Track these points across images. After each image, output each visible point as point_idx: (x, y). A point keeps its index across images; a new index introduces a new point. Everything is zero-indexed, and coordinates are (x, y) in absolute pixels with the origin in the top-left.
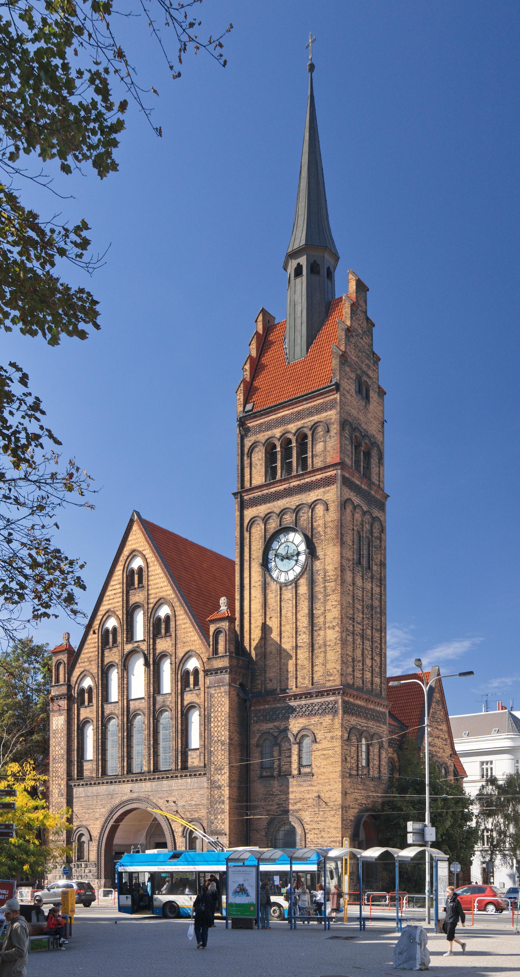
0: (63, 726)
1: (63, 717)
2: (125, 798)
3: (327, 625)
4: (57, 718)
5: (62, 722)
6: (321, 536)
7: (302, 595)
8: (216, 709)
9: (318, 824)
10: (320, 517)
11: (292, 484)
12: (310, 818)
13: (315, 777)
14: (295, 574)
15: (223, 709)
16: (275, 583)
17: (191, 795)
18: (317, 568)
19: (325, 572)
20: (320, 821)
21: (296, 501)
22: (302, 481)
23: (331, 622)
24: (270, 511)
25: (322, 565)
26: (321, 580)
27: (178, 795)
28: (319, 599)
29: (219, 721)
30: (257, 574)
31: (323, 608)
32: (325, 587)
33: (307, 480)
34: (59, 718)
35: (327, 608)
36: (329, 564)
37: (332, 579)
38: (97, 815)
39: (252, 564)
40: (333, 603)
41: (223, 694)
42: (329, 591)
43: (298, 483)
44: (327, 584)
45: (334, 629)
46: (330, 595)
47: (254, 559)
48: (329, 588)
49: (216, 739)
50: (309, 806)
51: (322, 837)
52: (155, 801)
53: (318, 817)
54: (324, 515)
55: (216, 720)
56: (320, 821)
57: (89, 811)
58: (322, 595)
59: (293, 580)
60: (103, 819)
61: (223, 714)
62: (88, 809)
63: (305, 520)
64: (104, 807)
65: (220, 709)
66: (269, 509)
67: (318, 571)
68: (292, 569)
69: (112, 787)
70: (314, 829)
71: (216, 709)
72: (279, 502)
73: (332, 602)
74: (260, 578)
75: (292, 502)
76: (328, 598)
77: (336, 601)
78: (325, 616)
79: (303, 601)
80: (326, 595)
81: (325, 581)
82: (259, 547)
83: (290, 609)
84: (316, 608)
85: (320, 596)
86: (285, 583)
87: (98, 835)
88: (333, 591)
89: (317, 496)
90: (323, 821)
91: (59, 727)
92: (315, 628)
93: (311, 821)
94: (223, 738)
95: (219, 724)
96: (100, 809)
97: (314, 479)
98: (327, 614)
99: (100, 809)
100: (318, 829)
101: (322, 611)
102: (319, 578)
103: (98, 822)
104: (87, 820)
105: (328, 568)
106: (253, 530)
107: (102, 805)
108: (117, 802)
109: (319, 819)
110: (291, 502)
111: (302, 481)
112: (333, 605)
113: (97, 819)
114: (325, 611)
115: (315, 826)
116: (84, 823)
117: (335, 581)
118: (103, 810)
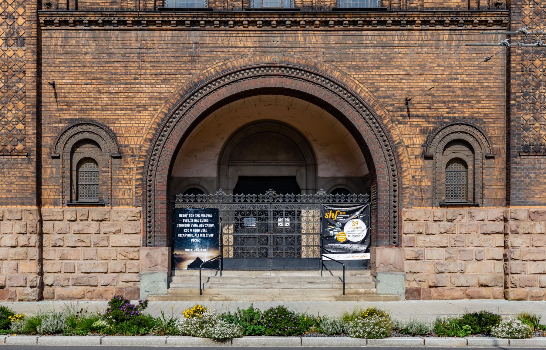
2: (239, 63)
17: (451, 66)
27: (411, 65)
38: (144, 100)
52: (336, 74)
57: (113, 88)
60: (163, 109)
62: (109, 83)
64: (165, 81)
87: (147, 146)
96: (151, 84)
99: (151, 84)
103: (145, 115)
104: (103, 109)
107: (158, 75)
108: (212, 70)
113: (143, 108)
116: (95, 115)
118: (164, 88)
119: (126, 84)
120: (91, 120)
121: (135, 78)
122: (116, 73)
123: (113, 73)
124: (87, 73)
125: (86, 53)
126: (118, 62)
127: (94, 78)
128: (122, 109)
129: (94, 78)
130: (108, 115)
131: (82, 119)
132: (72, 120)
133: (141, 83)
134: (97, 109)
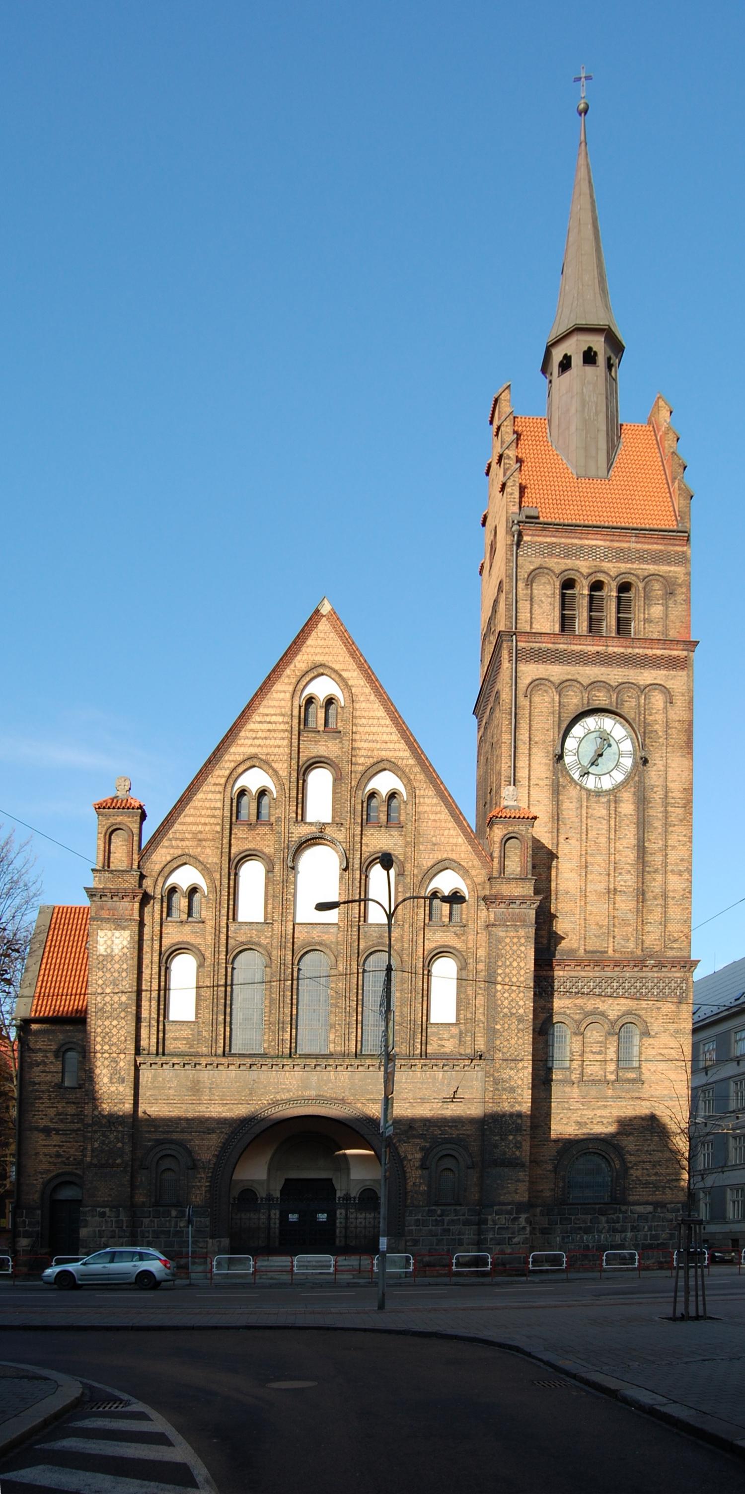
3: (669, 868)
6: (659, 738)
7: (625, 815)
9: (650, 1154)
10: (659, 710)
11: (611, 650)
12: (636, 1146)
13: (645, 1085)
14: (614, 782)
16: (578, 787)
18: (652, 783)
19: (667, 791)
20: (654, 1151)
21: (618, 675)
22: (630, 650)
23: (677, 864)
24: (570, 677)
25: (661, 779)
26: (659, 801)
28: (655, 828)
30: (544, 768)
31: (661, 843)
32: (666, 812)
33: (637, 651)
35: (670, 843)
36: (675, 781)
37: (678, 803)
39: (534, 750)
40: (681, 838)
42: (673, 819)
43: (622, 650)
44: (670, 809)
45: (681, 875)
46: (674, 825)
47: (536, 743)
50: (635, 1129)
51: (656, 1174)
53: (649, 1145)
54: (665, 708)
56: (654, 1151)
58: (660, 823)
59: (610, 790)
63: (631, 707)
66: (568, 674)
67: (654, 786)
68: (609, 773)
70: (644, 1162)
72: (587, 668)
73: (678, 835)
74: (549, 774)
75: (615, 675)
76: (671, 829)
77: (685, 836)
78: (666, 855)
80: (666, 825)
81: (666, 805)
82: (547, 727)
83: (604, 832)
84: (649, 840)
85: (658, 824)
86: (594, 792)
88: (681, 821)
89: (655, 679)
90: (658, 1151)
92: (647, 869)
93: (638, 1150)
97: (649, 652)
98: (669, 852)
100: (650, 1162)
101: (660, 845)
102: (657, 797)
105: (671, 785)
106: (536, 699)
109: (651, 1148)
110: (608, 675)
111: (630, 650)
112: (679, 841)
114: (666, 846)
115: (644, 1157)
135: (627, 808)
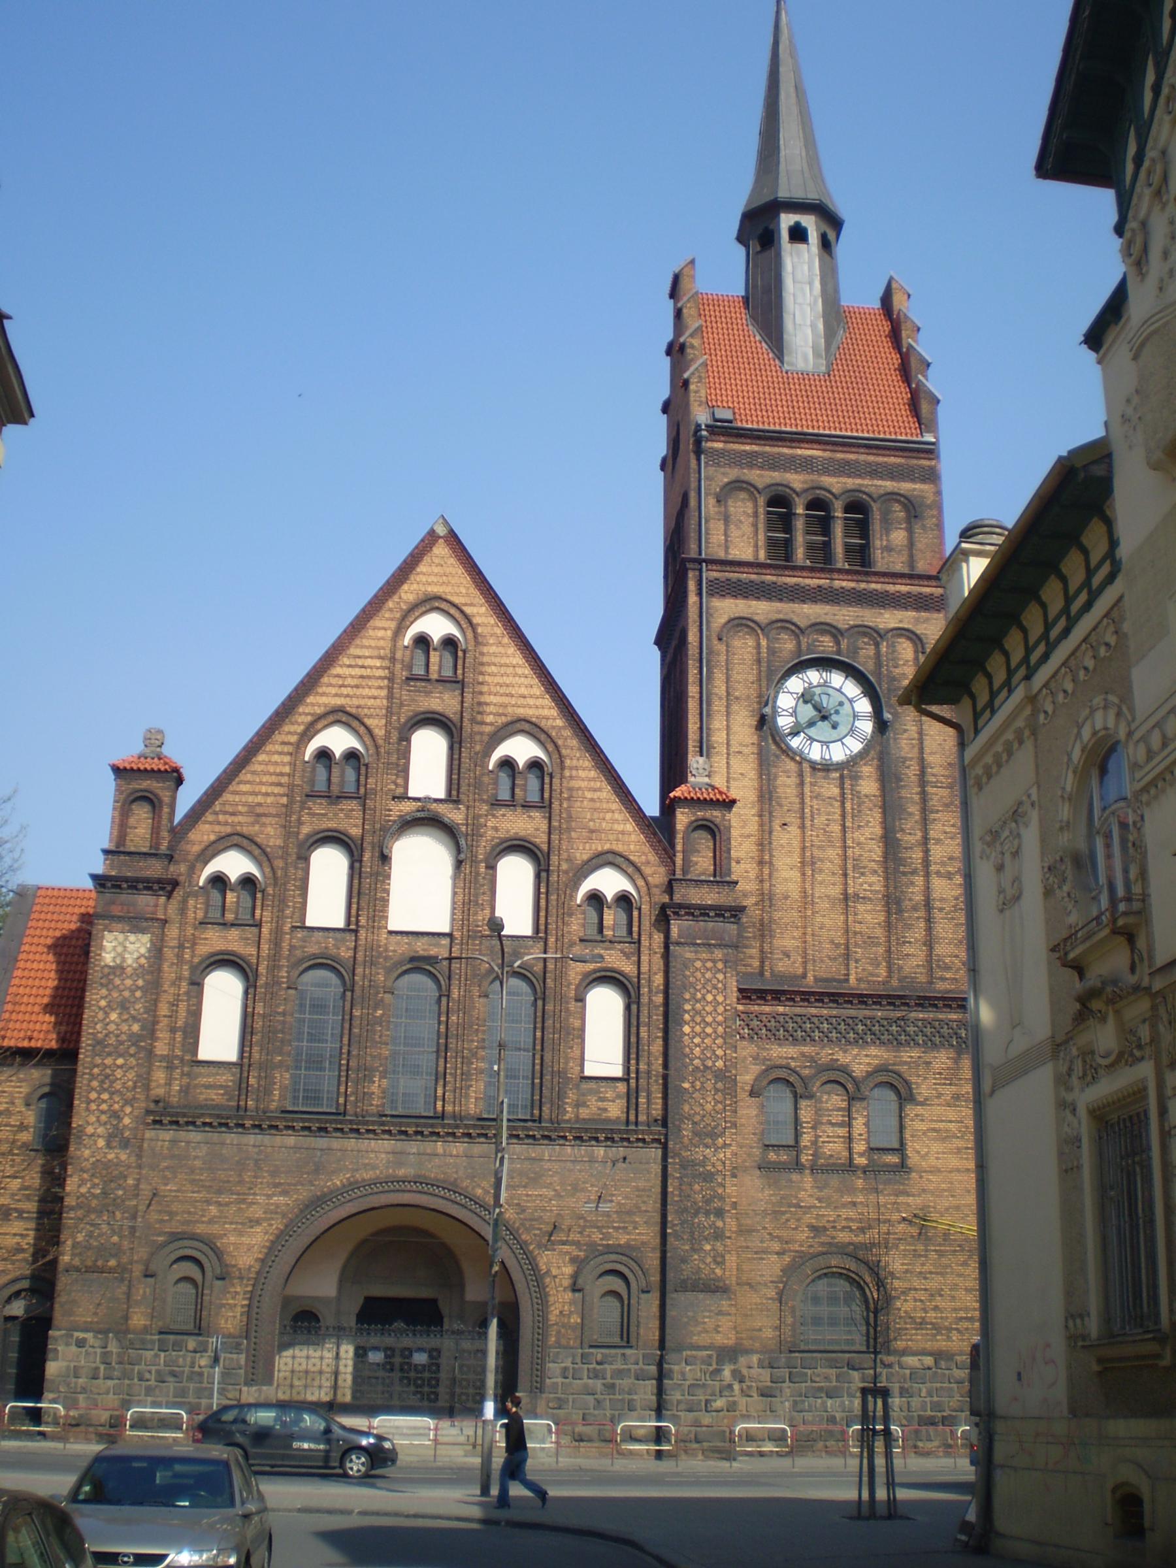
0: (143, 961)
1: (146, 939)
4: (121, 937)
5: (143, 950)
7: (866, 796)
8: (699, 996)
15: (720, 998)
28: (911, 814)
29: (708, 1024)
34: (132, 938)
41: (720, 965)
42: (934, 802)
46: (937, 812)
48: (936, 798)
49: (696, 1062)
55: (698, 1019)
57: (223, 1198)
61: (720, 1009)
65: (709, 997)
69: (322, 1142)
71: (699, 996)
76: (933, 816)
77: (953, 826)
79: (871, 810)
88: (947, 805)
91: (129, 962)
94: (720, 1064)
95: (709, 1030)
104: (211, 1222)
116: (200, 1229)
117: (950, 787)
119: (239, 1194)
120: (194, 1234)
121: (251, 1189)
122: (228, 1182)
123: (224, 1182)
124: (194, 1180)
125: (196, 1157)
126: (231, 1170)
127: (203, 1186)
128: (231, 1223)
129: (203, 1186)
130: (215, 1229)
131: (185, 1233)
132: (173, 1233)
133: (255, 1194)
134: (203, 1222)
135: (869, 786)
